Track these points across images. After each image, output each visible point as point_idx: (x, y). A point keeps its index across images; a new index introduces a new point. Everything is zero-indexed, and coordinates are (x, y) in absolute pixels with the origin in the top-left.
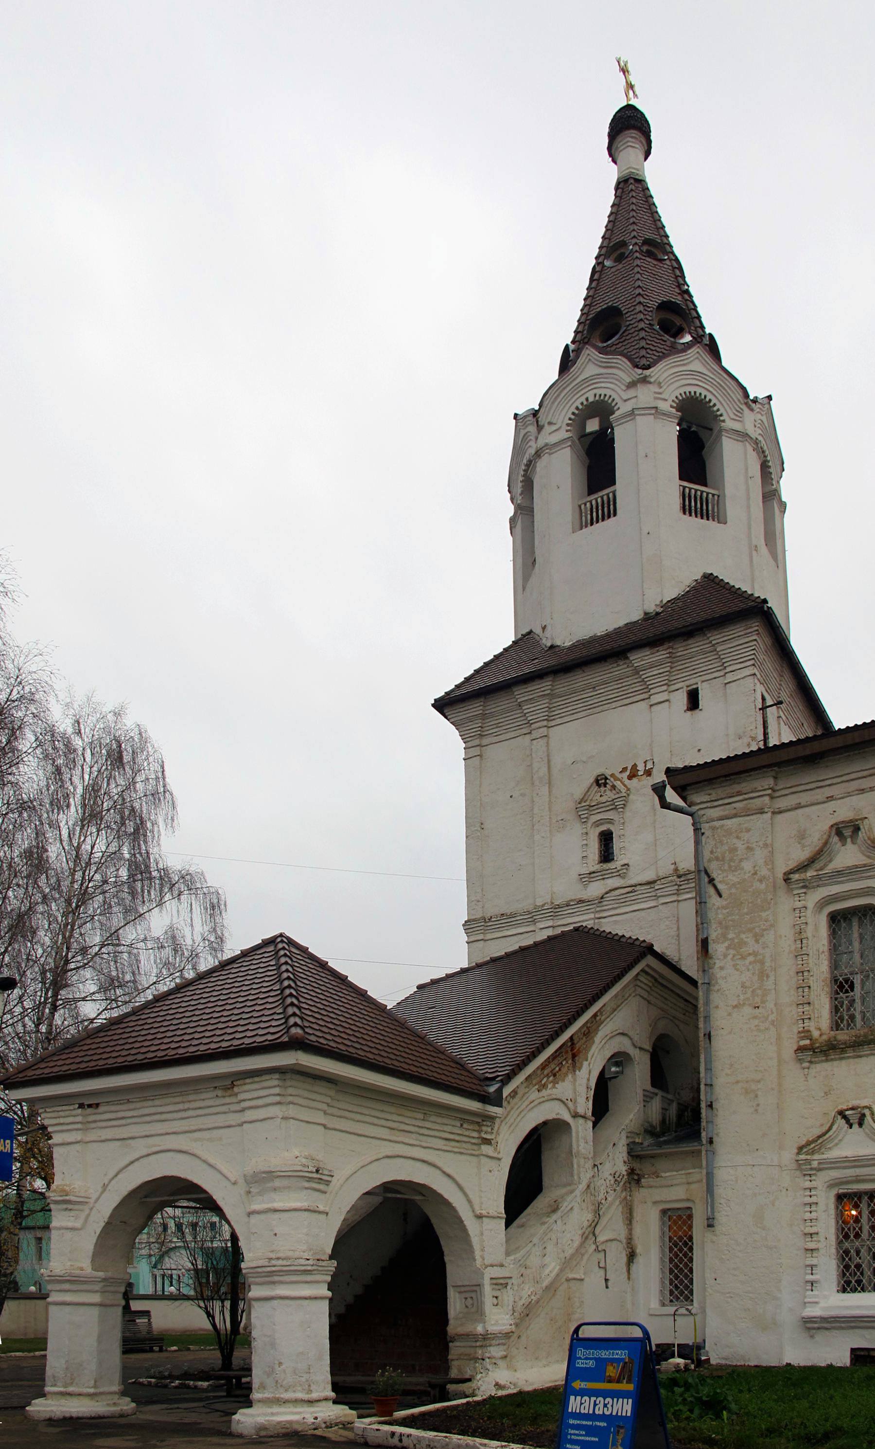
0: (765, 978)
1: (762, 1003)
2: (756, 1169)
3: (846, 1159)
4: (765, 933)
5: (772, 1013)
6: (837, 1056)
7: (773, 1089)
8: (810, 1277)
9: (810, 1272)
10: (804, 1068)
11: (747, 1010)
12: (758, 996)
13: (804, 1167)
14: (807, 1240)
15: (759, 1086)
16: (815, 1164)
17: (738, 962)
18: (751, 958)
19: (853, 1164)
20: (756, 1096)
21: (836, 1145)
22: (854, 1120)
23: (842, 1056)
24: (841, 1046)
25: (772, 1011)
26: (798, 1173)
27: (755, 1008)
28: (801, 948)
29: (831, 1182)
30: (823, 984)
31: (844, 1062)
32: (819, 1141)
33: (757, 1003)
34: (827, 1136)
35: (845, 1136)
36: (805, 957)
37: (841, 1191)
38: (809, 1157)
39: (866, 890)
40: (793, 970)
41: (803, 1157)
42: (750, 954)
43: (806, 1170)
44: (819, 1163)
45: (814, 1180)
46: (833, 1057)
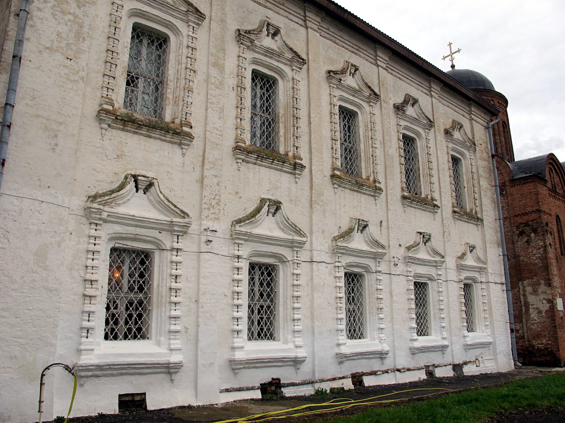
0: (81, 40)
1: (75, 57)
2: (43, 205)
3: (133, 218)
4: (87, 5)
5: (83, 70)
6: (133, 130)
7: (73, 135)
8: (86, 324)
9: (87, 318)
10: (102, 129)
11: (59, 57)
12: (72, 50)
13: (94, 216)
14: (87, 286)
15: (60, 128)
16: (105, 215)
17: (59, 14)
18: (71, 17)
19: (137, 223)
20: (56, 136)
21: (124, 203)
22: (142, 186)
23: (137, 131)
24: (140, 123)
25: (83, 68)
26: (84, 220)
27: (68, 58)
28: (114, 34)
29: (113, 235)
30: (123, 70)
31: (136, 136)
32: (113, 196)
33: (71, 56)
34: (121, 192)
35: (132, 197)
36: (116, 42)
37: (117, 245)
38: (101, 207)
39: (168, 22)
40: (104, 47)
41: (96, 205)
42: (70, 13)
43: (95, 219)
44: (108, 216)
45: (100, 230)
46: (129, 129)
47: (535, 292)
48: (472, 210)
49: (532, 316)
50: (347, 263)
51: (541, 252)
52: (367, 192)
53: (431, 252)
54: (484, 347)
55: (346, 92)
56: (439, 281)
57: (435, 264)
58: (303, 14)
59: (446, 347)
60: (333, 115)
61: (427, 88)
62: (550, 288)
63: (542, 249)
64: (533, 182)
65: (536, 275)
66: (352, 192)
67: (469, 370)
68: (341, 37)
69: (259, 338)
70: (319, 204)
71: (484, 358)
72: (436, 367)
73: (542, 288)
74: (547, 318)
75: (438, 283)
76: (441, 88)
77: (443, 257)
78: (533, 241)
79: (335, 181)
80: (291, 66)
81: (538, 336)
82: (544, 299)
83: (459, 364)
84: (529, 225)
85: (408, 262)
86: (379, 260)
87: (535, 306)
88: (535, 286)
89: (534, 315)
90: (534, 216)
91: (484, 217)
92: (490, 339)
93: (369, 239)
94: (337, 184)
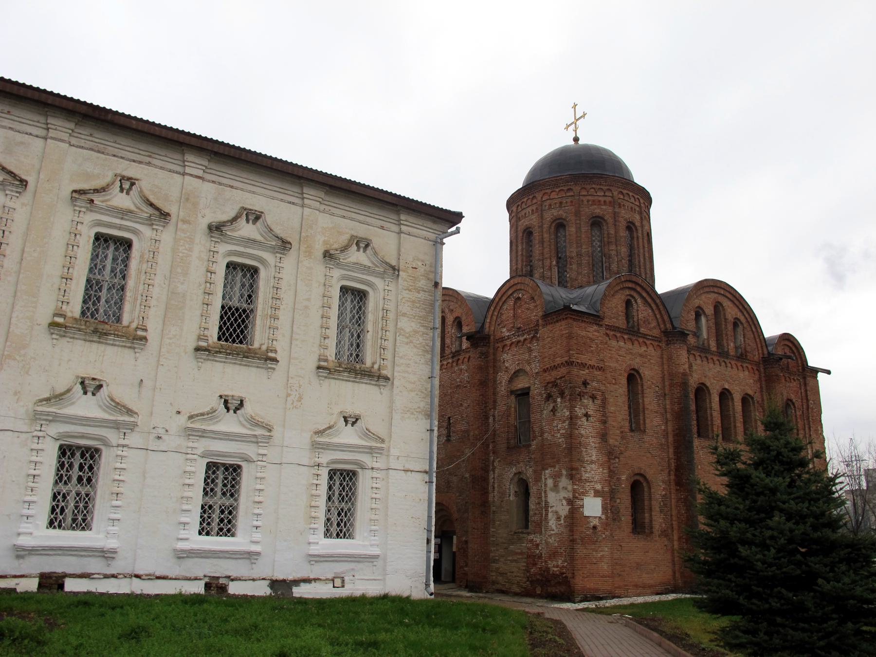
47: (556, 488)
48: (373, 364)
49: (550, 524)
50: (59, 433)
51: (566, 427)
52: (117, 343)
53: (245, 423)
54: (358, 562)
55: (108, 215)
56: (259, 462)
57: (254, 440)
58: (44, 121)
59: (258, 554)
60: (71, 247)
61: (297, 195)
62: (571, 481)
63: (567, 422)
64: (566, 318)
65: (558, 462)
66: (88, 344)
67: (300, 591)
68: (115, 142)
69: (51, 527)
70: (15, 359)
71: (356, 577)
72: (232, 580)
73: (564, 482)
74: (566, 527)
75: (257, 465)
76: (325, 193)
77: (270, 431)
78: (559, 410)
79: (52, 331)
80: (5, 190)
81: (554, 555)
82: (564, 498)
83: (284, 581)
84: (556, 386)
85: (189, 435)
86: (124, 431)
87: (554, 509)
88: (556, 477)
89: (552, 523)
90: (563, 370)
91: (396, 374)
92: (375, 551)
93: (104, 403)
94: (57, 334)
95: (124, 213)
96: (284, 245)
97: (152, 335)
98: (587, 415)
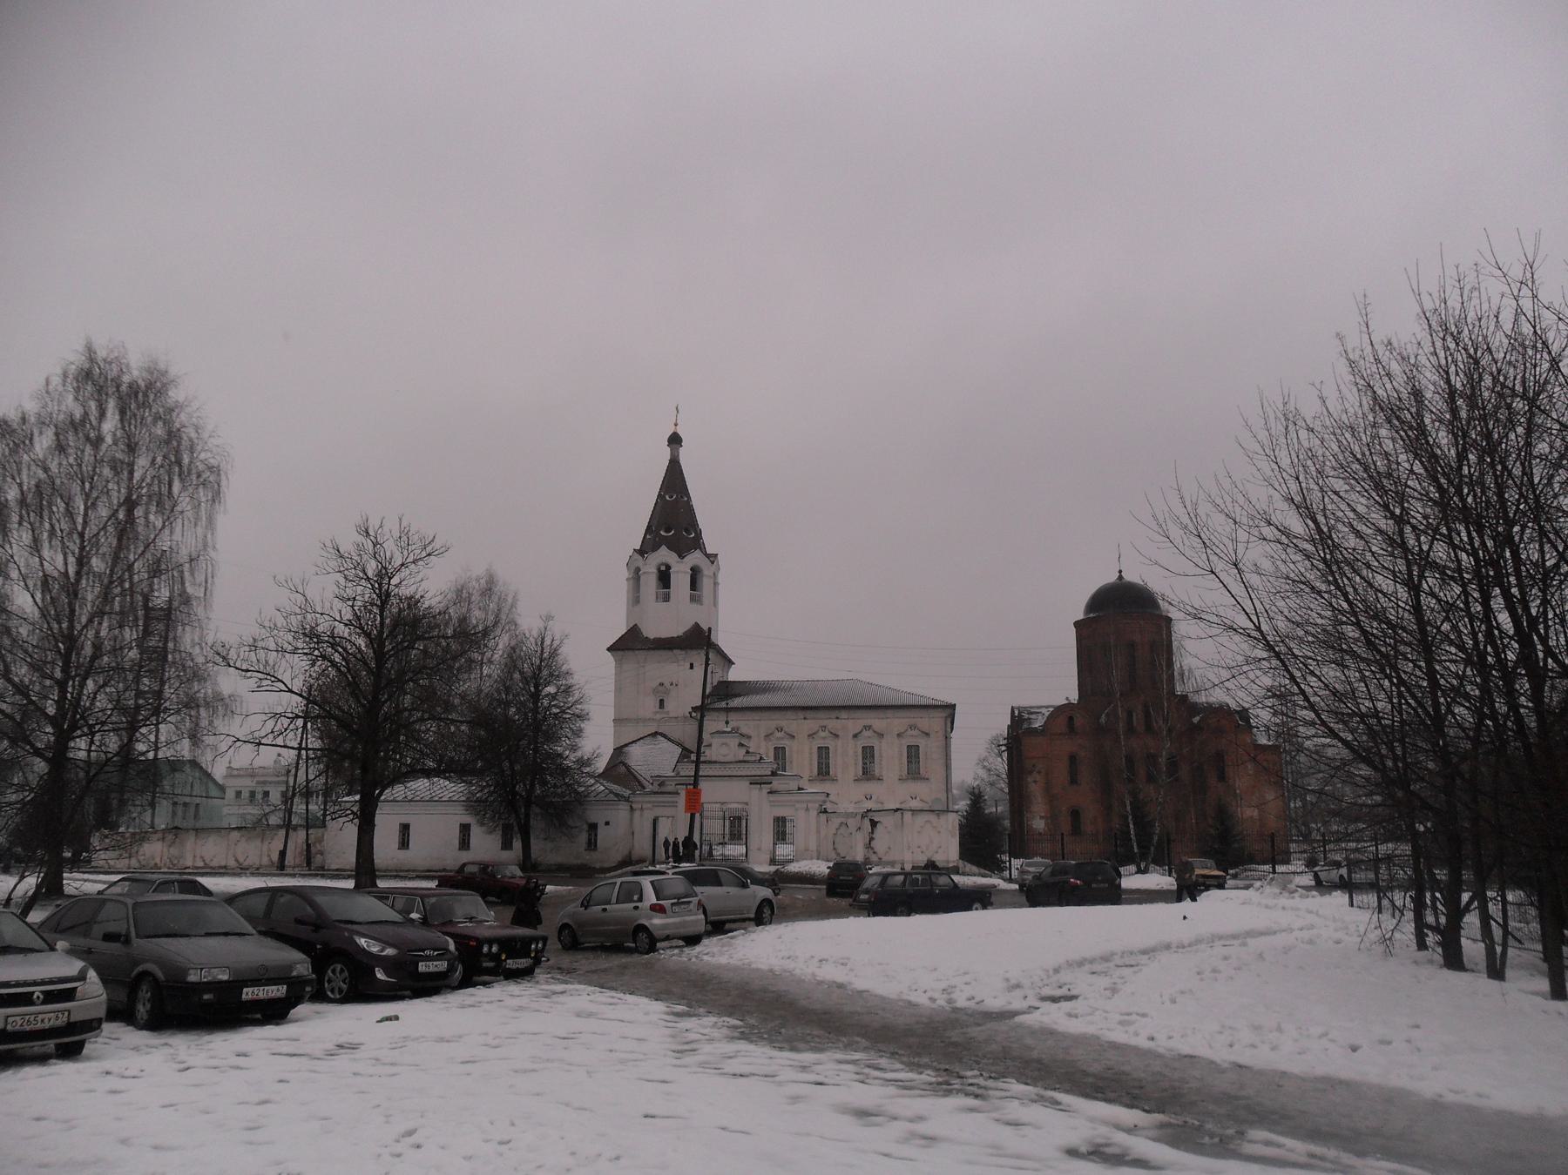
95: (824, 738)
96: (881, 735)
97: (839, 776)
98: (1035, 782)
